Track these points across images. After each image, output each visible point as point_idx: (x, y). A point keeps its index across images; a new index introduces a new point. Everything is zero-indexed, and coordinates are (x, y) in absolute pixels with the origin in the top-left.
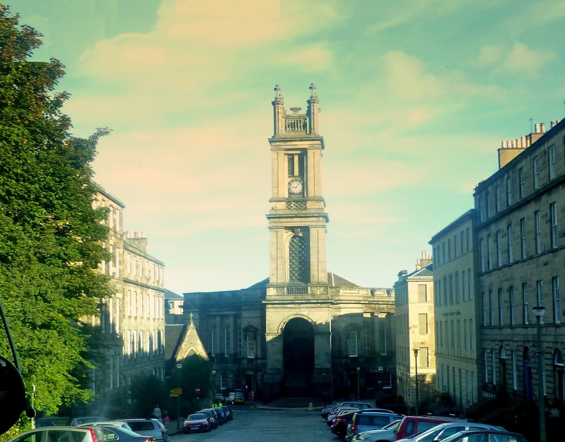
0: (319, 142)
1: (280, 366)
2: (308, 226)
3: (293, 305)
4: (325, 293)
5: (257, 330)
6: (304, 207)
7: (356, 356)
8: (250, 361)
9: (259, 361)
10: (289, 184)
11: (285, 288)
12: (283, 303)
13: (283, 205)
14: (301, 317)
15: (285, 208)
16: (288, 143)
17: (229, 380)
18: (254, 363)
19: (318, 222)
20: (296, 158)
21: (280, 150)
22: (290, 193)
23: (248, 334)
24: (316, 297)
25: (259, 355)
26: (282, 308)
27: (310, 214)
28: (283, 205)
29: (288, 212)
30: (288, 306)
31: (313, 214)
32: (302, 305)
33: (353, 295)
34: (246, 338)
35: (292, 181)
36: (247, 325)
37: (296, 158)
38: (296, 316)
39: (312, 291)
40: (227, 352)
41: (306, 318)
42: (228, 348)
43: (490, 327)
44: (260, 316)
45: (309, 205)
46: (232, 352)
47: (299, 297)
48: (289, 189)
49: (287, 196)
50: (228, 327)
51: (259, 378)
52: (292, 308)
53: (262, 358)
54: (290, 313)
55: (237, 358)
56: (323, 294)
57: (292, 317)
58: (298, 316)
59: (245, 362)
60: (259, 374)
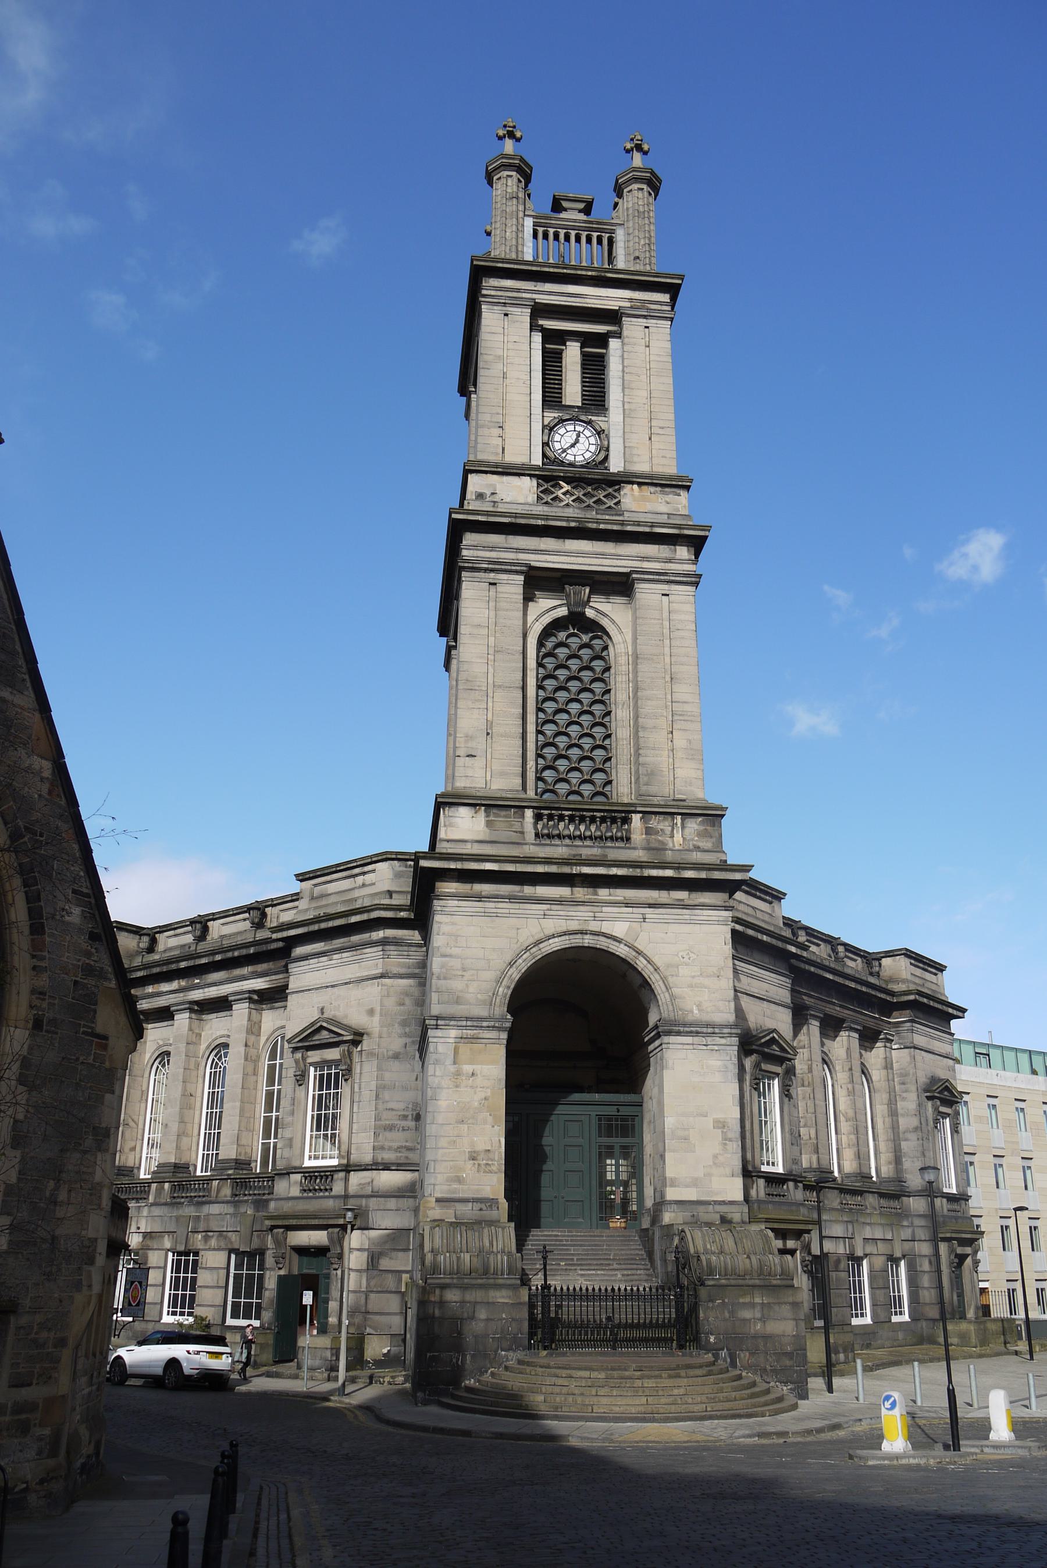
0: (665, 298)
2: (627, 575)
3: (563, 891)
4: (707, 844)
6: (611, 503)
7: (780, 1169)
8: (317, 1179)
10: (549, 429)
11: (529, 813)
14: (603, 943)
15: (532, 498)
16: (549, 287)
17: (204, 1277)
18: (338, 1188)
19: (670, 561)
20: (572, 353)
21: (517, 303)
23: (314, 1056)
24: (669, 856)
26: (511, 898)
27: (638, 524)
29: (541, 509)
30: (543, 891)
31: (653, 525)
32: (604, 893)
33: (759, 914)
34: (301, 1079)
35: (562, 421)
36: (316, 1015)
37: (572, 353)
39: (648, 831)
40: (206, 1158)
41: (621, 950)
42: (214, 1140)
44: (380, 971)
46: (228, 1151)
47: (589, 851)
48: (546, 444)
49: (537, 460)
50: (221, 1048)
51: (355, 1260)
52: (560, 901)
54: (551, 926)
56: (697, 848)
58: (588, 941)
59: (289, 1188)
60: (355, 1239)
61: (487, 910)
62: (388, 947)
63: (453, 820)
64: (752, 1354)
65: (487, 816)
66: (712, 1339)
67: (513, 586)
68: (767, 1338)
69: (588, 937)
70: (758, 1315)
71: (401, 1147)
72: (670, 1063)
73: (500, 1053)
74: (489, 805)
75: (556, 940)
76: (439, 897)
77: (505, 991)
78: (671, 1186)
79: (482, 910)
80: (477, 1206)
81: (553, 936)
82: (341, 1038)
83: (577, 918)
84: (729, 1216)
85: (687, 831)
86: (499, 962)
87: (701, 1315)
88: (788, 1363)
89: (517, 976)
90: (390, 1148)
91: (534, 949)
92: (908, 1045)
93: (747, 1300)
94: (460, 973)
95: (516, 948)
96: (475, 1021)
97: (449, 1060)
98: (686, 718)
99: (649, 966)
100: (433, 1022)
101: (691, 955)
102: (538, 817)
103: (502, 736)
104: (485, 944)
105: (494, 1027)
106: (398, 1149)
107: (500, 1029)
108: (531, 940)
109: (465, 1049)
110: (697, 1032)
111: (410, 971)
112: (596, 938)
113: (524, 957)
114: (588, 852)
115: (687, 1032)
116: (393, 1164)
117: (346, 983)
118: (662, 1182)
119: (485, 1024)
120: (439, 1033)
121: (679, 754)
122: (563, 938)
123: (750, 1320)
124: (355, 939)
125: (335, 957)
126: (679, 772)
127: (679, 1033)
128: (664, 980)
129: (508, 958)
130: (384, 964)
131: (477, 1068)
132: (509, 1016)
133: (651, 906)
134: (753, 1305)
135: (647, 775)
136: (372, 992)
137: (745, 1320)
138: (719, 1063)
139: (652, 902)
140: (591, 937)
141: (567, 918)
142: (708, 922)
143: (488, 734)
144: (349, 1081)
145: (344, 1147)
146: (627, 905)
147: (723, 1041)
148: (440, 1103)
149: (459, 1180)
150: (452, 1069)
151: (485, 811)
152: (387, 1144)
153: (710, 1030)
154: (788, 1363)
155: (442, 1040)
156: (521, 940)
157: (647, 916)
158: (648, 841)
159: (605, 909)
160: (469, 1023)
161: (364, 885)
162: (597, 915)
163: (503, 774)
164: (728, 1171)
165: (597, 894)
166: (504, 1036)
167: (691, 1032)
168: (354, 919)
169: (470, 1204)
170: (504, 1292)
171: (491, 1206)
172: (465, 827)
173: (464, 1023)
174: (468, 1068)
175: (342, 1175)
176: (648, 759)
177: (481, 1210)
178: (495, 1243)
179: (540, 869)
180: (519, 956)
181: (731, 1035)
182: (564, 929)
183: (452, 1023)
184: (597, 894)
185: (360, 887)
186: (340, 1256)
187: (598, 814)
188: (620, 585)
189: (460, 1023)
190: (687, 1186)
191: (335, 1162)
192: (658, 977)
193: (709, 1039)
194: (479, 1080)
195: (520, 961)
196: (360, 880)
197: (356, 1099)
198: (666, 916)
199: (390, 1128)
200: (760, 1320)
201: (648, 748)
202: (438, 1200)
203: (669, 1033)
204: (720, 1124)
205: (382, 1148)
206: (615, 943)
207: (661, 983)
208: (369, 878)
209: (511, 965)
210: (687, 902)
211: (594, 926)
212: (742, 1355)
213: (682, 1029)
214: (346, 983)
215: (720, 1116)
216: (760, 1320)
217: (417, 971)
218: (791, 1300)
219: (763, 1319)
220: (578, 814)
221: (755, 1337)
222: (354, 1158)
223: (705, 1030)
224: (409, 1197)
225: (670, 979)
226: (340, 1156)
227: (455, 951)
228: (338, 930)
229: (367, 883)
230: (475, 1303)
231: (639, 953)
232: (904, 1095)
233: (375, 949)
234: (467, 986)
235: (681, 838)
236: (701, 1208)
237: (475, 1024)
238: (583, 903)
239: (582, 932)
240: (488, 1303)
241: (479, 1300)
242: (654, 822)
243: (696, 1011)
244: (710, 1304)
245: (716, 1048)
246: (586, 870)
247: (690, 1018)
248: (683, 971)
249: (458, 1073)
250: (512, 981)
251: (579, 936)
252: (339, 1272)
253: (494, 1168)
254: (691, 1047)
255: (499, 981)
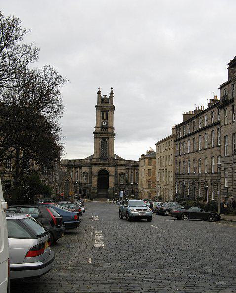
1: (96, 187)
12: (98, 165)
13: (99, 130)
20: (105, 113)
22: (102, 125)
28: (99, 130)
29: (101, 132)
37: (105, 113)
43: (179, 174)
45: (109, 130)
46: (78, 181)
47: (104, 162)
55: (80, 183)
67: (98, 139)
74: (96, 159)
83: (103, 167)
104: (96, 170)
188: (108, 138)
228: (86, 165)
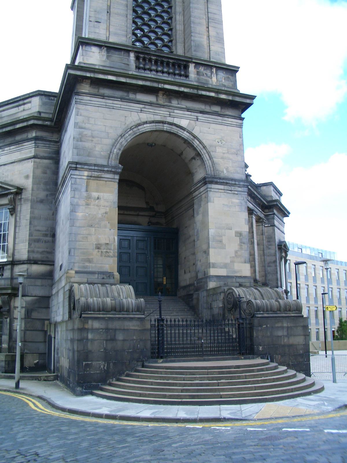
3: (151, 98)
5: (20, 191)
9: (19, 269)
11: (132, 55)
14: (174, 129)
18: (7, 274)
25: (23, 253)
26: (122, 99)
30: (140, 97)
32: (175, 103)
38: (160, 127)
39: (198, 73)
41: (185, 135)
44: (32, 154)
51: (18, 313)
52: (151, 104)
53: (30, 261)
54: (145, 117)
57: (147, 127)
58: (166, 127)
61: (107, 104)
62: (38, 142)
63: (88, 53)
64: (282, 356)
65: (108, 52)
66: (261, 348)
68: (290, 346)
69: (166, 125)
70: (285, 334)
71: (44, 251)
72: (212, 199)
73: (115, 187)
75: (148, 125)
76: (78, 94)
77: (117, 151)
78: (213, 267)
79: (105, 104)
80: (102, 276)
81: (146, 123)
82: (9, 191)
83: (161, 114)
84: (244, 284)
85: (219, 77)
86: (114, 134)
87: (255, 334)
88: (301, 360)
89: (125, 143)
90: (38, 252)
91: (135, 129)
92: (272, 225)
93: (279, 325)
94: (90, 139)
95: (124, 127)
96: (100, 168)
97: (84, 189)
98: (215, 21)
99: (200, 145)
100: (75, 166)
101: (223, 141)
102: (137, 58)
103: (116, 14)
105: (111, 171)
106: (42, 253)
107: (115, 173)
108: (133, 124)
109: (93, 183)
110: (227, 183)
111: (50, 155)
112: (171, 126)
113: (130, 133)
114: (166, 79)
115: (221, 182)
116: (39, 261)
117: (12, 163)
118: (208, 265)
119: (106, 169)
120: (77, 172)
121: (212, 39)
122: (152, 124)
123: (281, 336)
124: (18, 138)
125: (6, 149)
126: (212, 48)
127: (217, 183)
128: (208, 153)
129: (120, 132)
130: (35, 151)
131: (101, 195)
132: (120, 166)
133: (202, 112)
134: (282, 328)
135: (195, 46)
136: (29, 166)
137: (278, 336)
138: (237, 201)
139: (201, 110)
140: (168, 126)
141: (155, 114)
142: (231, 125)
143: (108, 12)
144: (14, 216)
145: (11, 251)
146: (188, 110)
147: (240, 189)
148: (77, 214)
149: (90, 261)
150: (85, 194)
151: (107, 50)
152: (36, 249)
153: (233, 182)
154: (301, 360)
155: (79, 177)
156: (127, 123)
157: (199, 118)
158: (198, 79)
159: (175, 111)
160: (96, 168)
161: (24, 110)
162: (171, 114)
163: (116, 34)
164: (243, 260)
165: (171, 103)
166: (117, 177)
167: (224, 183)
168: (18, 126)
169: (97, 275)
170: (135, 323)
171: (109, 276)
172: (94, 57)
173: (93, 168)
174: (95, 194)
175: (9, 267)
176: (196, 39)
177: (103, 278)
178: (121, 294)
179: (140, 83)
180: (126, 132)
181: (244, 186)
182: (153, 120)
183: (86, 167)
184: (171, 103)
185: (21, 111)
186: (9, 311)
187: (171, 61)
189: (90, 167)
190: (221, 268)
191: (5, 260)
192: (205, 151)
193: (233, 188)
194: (102, 202)
195: (127, 135)
196: (21, 108)
197: (18, 225)
198: (209, 119)
199: (38, 241)
200: (286, 336)
201: (196, 33)
202: (77, 272)
203: (211, 182)
204: (239, 234)
205: (33, 252)
206: (181, 130)
207: (207, 155)
208: (27, 106)
209: (122, 136)
210: (219, 113)
211: (169, 120)
212: (277, 357)
213: (218, 181)
214: (12, 163)
215: (238, 230)
216: (286, 336)
217: (54, 156)
218: (302, 324)
219: (288, 336)
220: (160, 59)
221: (284, 346)
222: (17, 257)
223: (231, 182)
224: (48, 279)
225: (212, 153)
226: (8, 257)
227: (87, 126)
229: (26, 109)
230: (115, 330)
231: (195, 137)
232: (270, 247)
233: (30, 143)
234: (95, 147)
235: (216, 79)
236: (229, 280)
237: (100, 168)
238: (163, 106)
239: (163, 122)
240: (124, 330)
241: (118, 327)
242: (201, 69)
243: (225, 172)
244: (260, 328)
245: (236, 193)
246: (167, 87)
247: (222, 175)
248: (218, 150)
249: (89, 197)
250: (122, 146)
251: (161, 124)
252: (8, 320)
253: (111, 254)
254: (223, 191)
255: (114, 145)
